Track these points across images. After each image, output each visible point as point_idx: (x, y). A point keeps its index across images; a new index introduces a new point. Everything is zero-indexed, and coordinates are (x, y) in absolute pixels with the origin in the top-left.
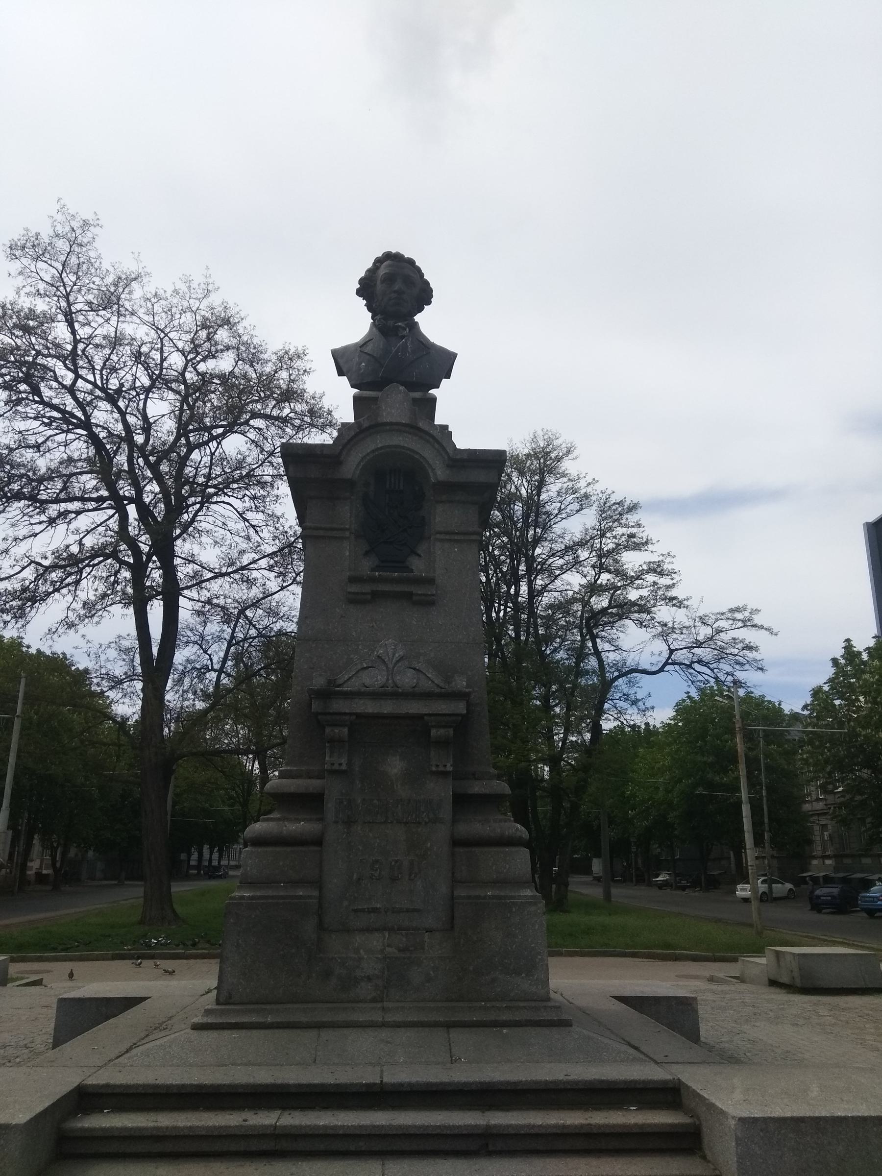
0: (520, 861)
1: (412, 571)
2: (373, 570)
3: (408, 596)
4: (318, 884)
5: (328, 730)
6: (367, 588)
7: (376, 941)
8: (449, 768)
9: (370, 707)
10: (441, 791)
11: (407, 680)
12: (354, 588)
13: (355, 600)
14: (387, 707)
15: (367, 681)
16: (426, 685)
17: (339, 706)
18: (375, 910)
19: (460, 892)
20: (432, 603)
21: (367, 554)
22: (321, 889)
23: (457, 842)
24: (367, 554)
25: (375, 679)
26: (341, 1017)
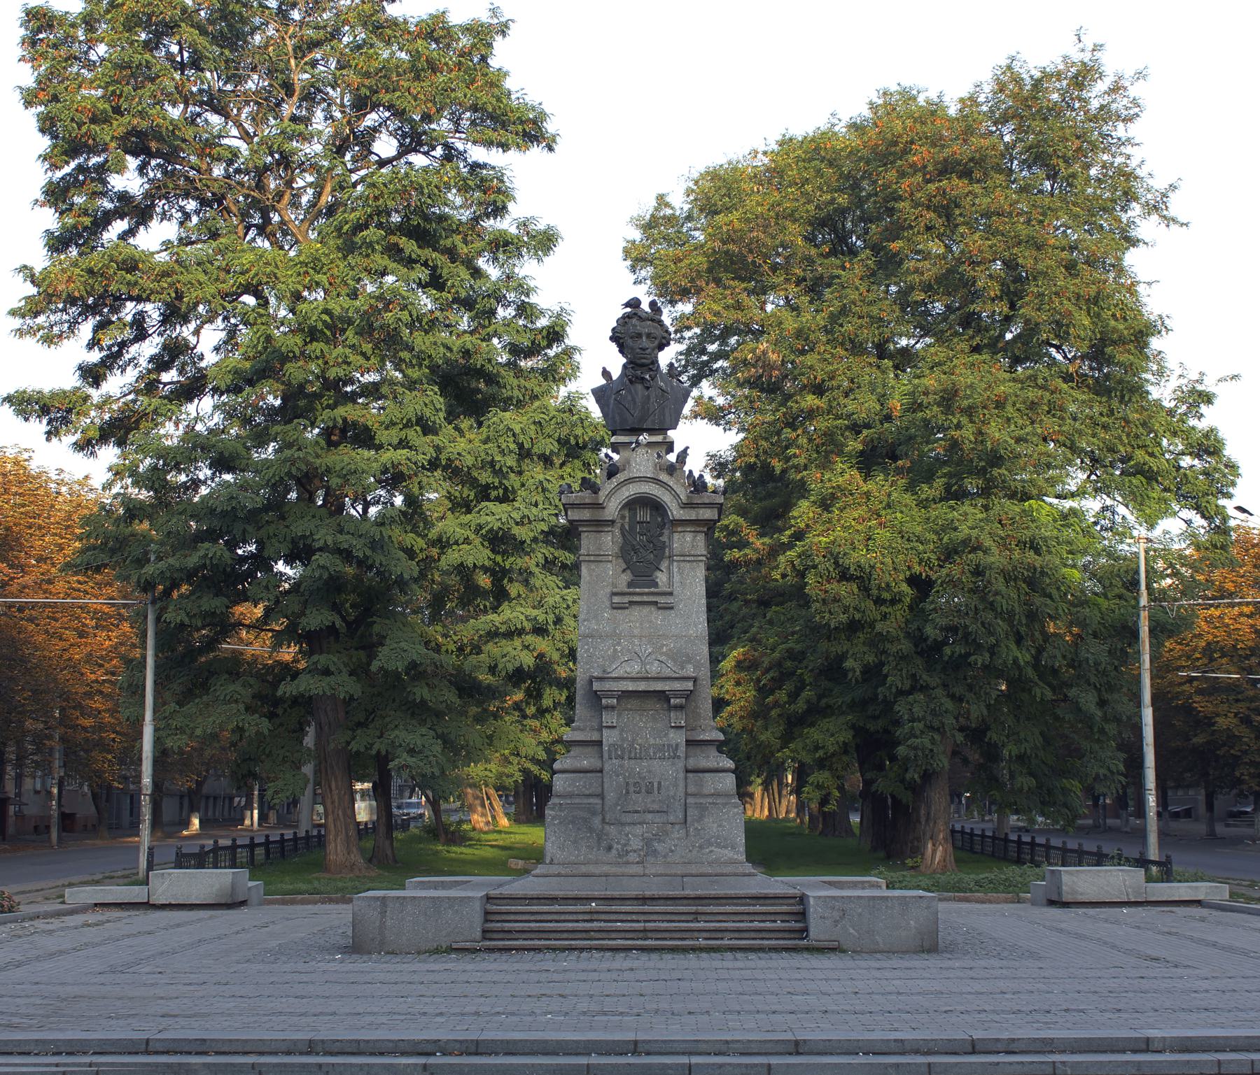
0: (729, 781)
1: (656, 585)
2: (630, 585)
3: (656, 603)
4: (602, 796)
5: (604, 701)
6: (626, 599)
7: (639, 830)
8: (683, 724)
9: (631, 686)
10: (679, 738)
11: (654, 669)
12: (616, 599)
13: (615, 607)
14: (642, 686)
15: (628, 670)
16: (667, 672)
17: (608, 686)
18: (637, 812)
19: (690, 800)
20: (672, 608)
21: (624, 571)
22: (603, 799)
23: (687, 771)
24: (624, 571)
25: (635, 668)
26: (619, 870)
